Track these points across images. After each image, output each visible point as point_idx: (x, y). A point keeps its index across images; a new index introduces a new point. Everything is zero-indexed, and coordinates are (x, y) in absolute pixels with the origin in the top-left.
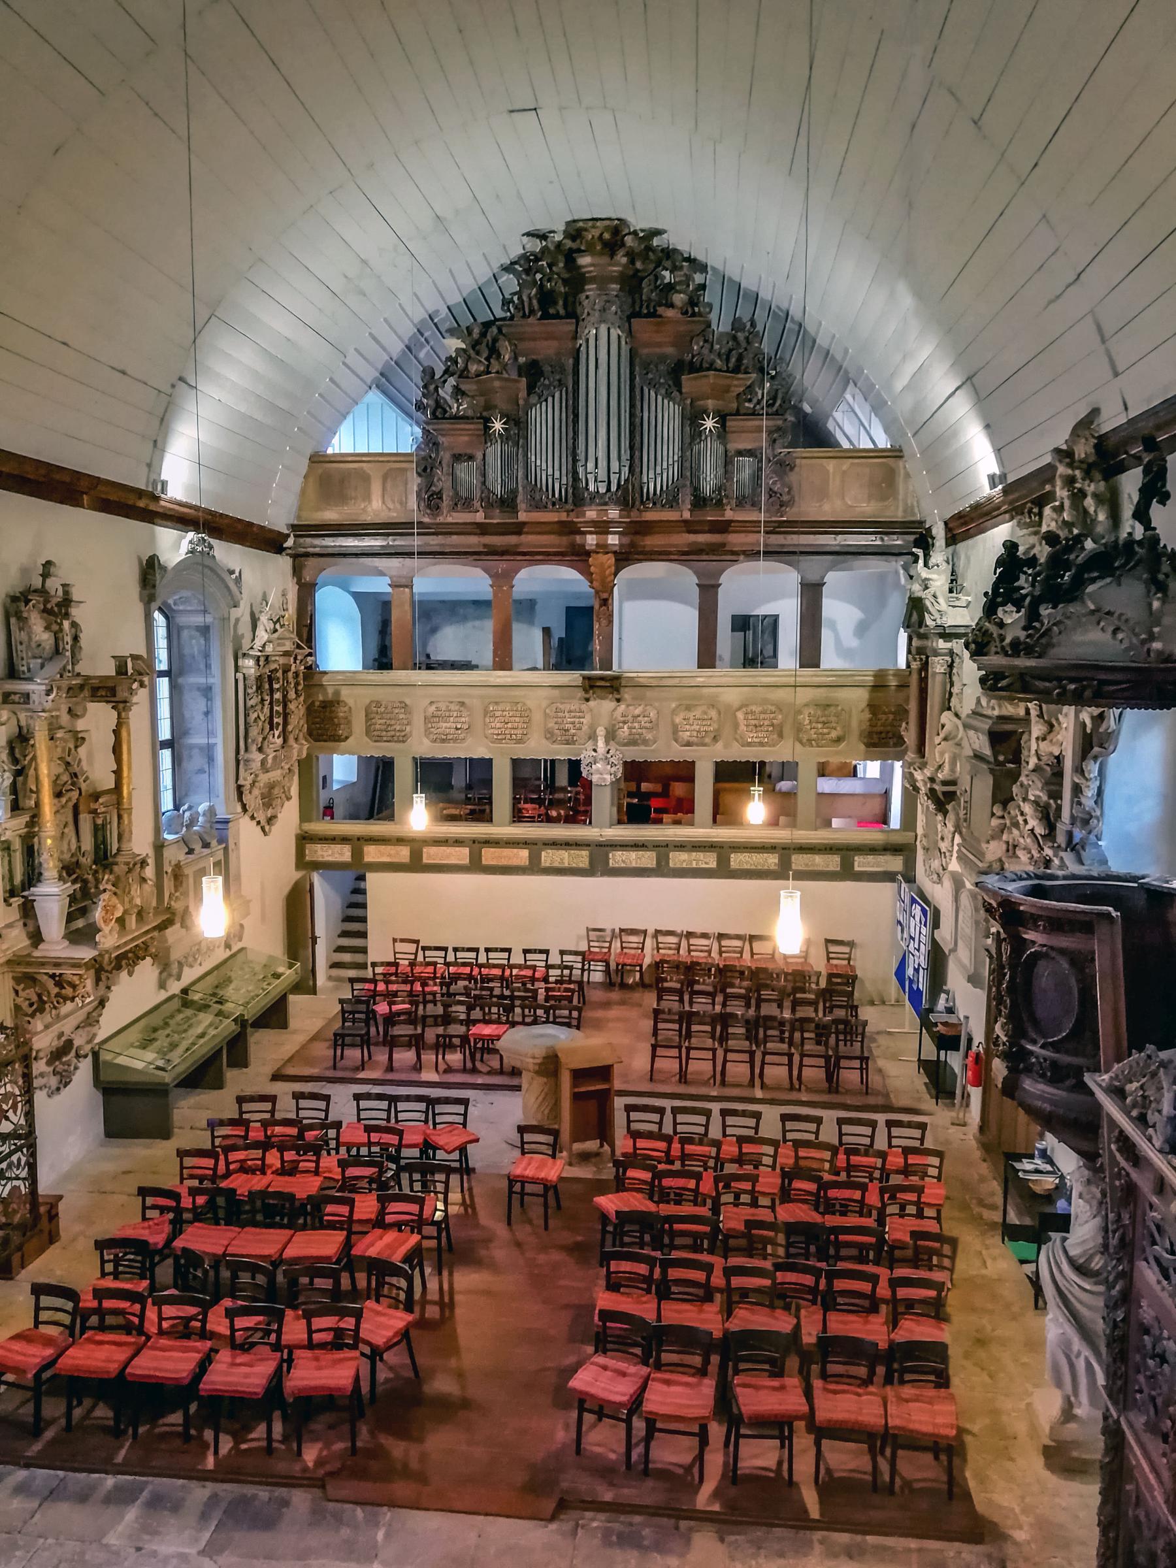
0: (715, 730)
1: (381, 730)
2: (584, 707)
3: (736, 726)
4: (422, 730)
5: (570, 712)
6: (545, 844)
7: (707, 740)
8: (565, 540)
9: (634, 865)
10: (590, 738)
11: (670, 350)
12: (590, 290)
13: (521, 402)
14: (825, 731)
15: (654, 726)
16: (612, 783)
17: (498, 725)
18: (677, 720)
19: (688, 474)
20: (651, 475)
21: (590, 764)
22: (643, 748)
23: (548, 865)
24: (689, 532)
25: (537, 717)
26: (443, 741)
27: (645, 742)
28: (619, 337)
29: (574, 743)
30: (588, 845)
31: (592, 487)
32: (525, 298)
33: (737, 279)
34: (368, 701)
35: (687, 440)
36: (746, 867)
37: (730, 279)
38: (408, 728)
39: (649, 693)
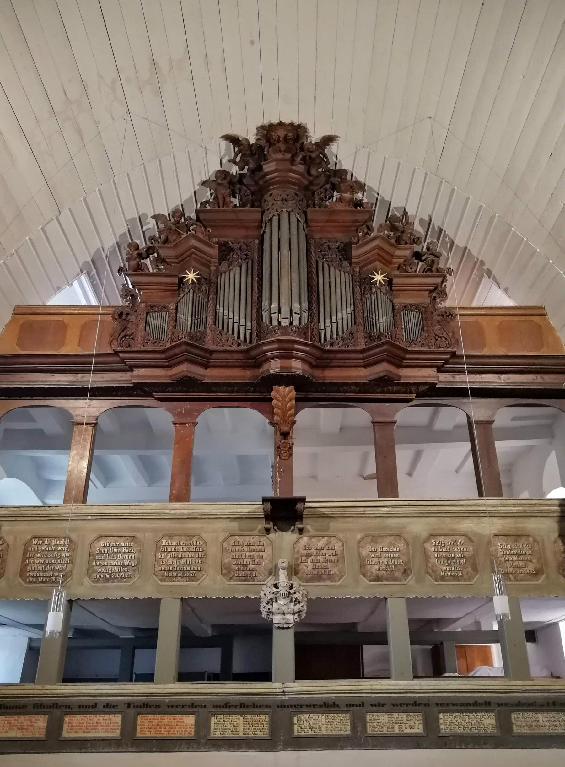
0: (406, 563)
1: (39, 571)
2: (263, 540)
3: (426, 557)
4: (85, 568)
5: (248, 545)
6: (215, 706)
7: (397, 574)
8: (248, 373)
9: (324, 732)
10: (270, 574)
11: (339, 235)
12: (273, 189)
13: (213, 268)
14: (521, 564)
15: (339, 558)
16: (296, 624)
17: (170, 560)
18: (364, 553)
19: (361, 321)
20: (328, 323)
21: (271, 602)
22: (328, 583)
23: (218, 735)
24: (365, 366)
25: (213, 551)
26: (107, 580)
27: (331, 577)
28: (298, 220)
29: (253, 578)
30: (267, 706)
31: (275, 323)
32: (220, 197)
33: (387, 198)
34: (29, 537)
35: (358, 297)
36: (460, 731)
37: (383, 200)
38: (69, 566)
39: (333, 525)
